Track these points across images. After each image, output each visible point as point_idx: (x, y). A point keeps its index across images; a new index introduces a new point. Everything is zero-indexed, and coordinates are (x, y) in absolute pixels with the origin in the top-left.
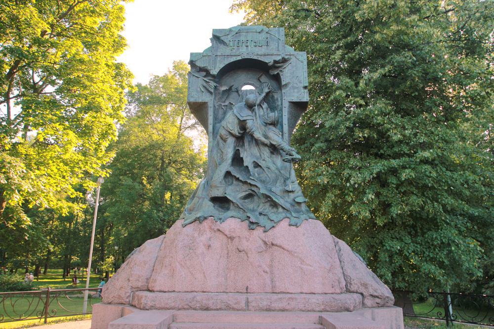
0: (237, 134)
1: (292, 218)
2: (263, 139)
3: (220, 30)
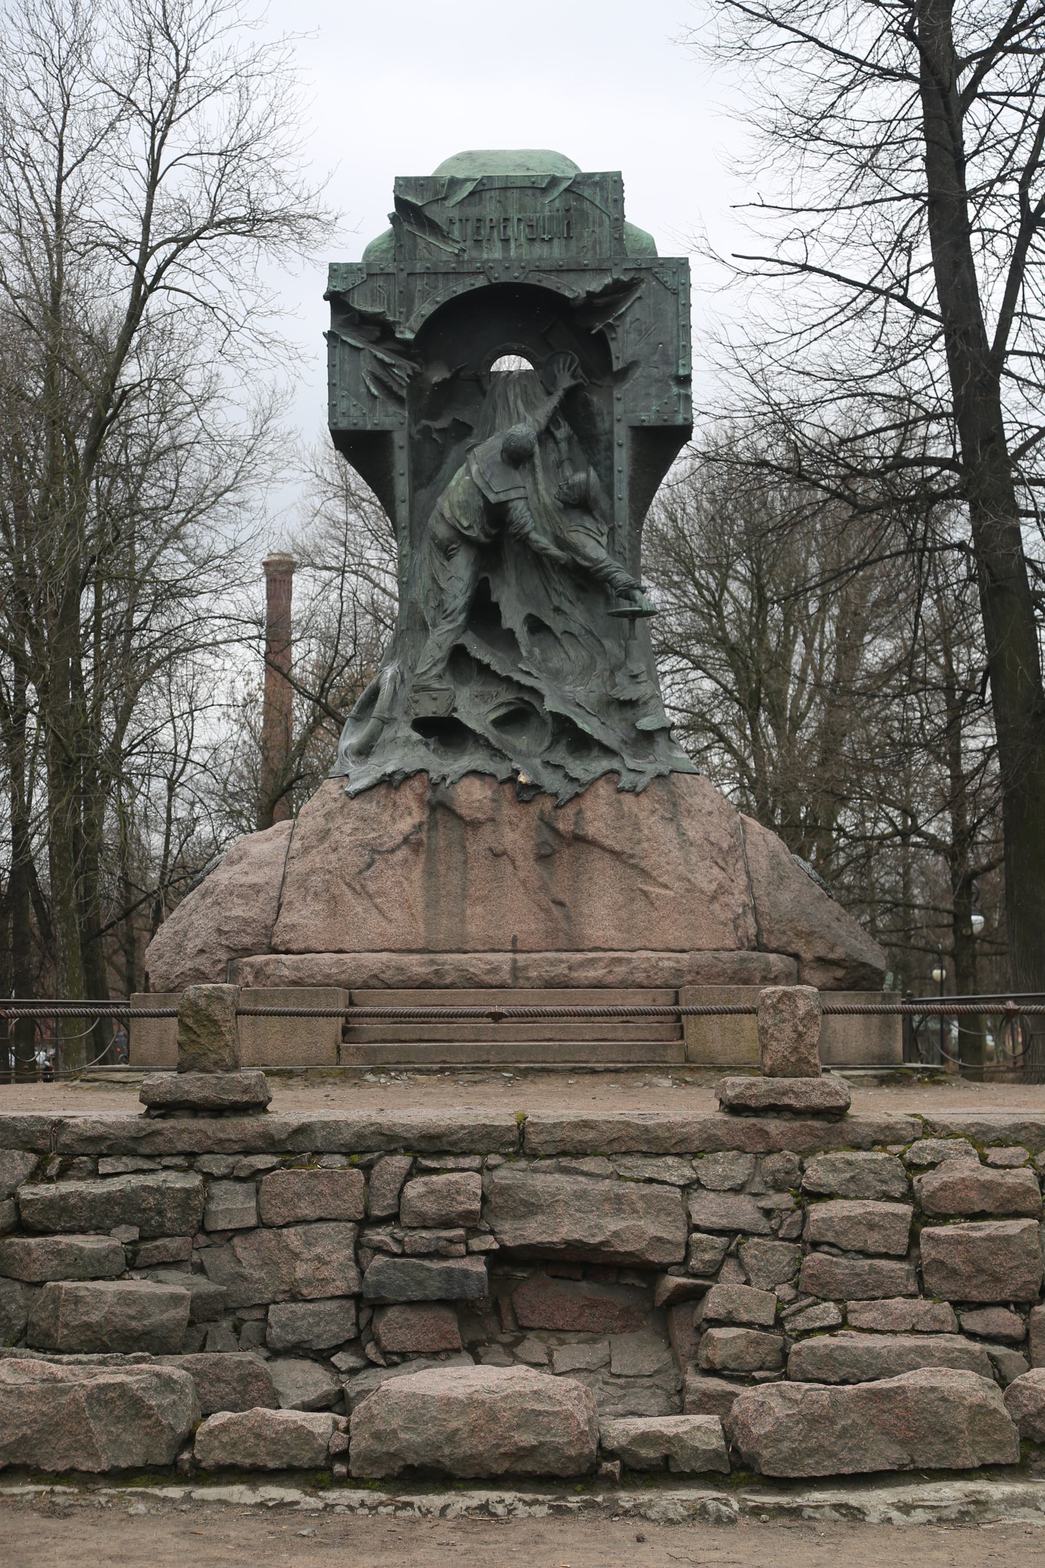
0: (483, 538)
1: (624, 772)
2: (554, 551)
3: (417, 179)
